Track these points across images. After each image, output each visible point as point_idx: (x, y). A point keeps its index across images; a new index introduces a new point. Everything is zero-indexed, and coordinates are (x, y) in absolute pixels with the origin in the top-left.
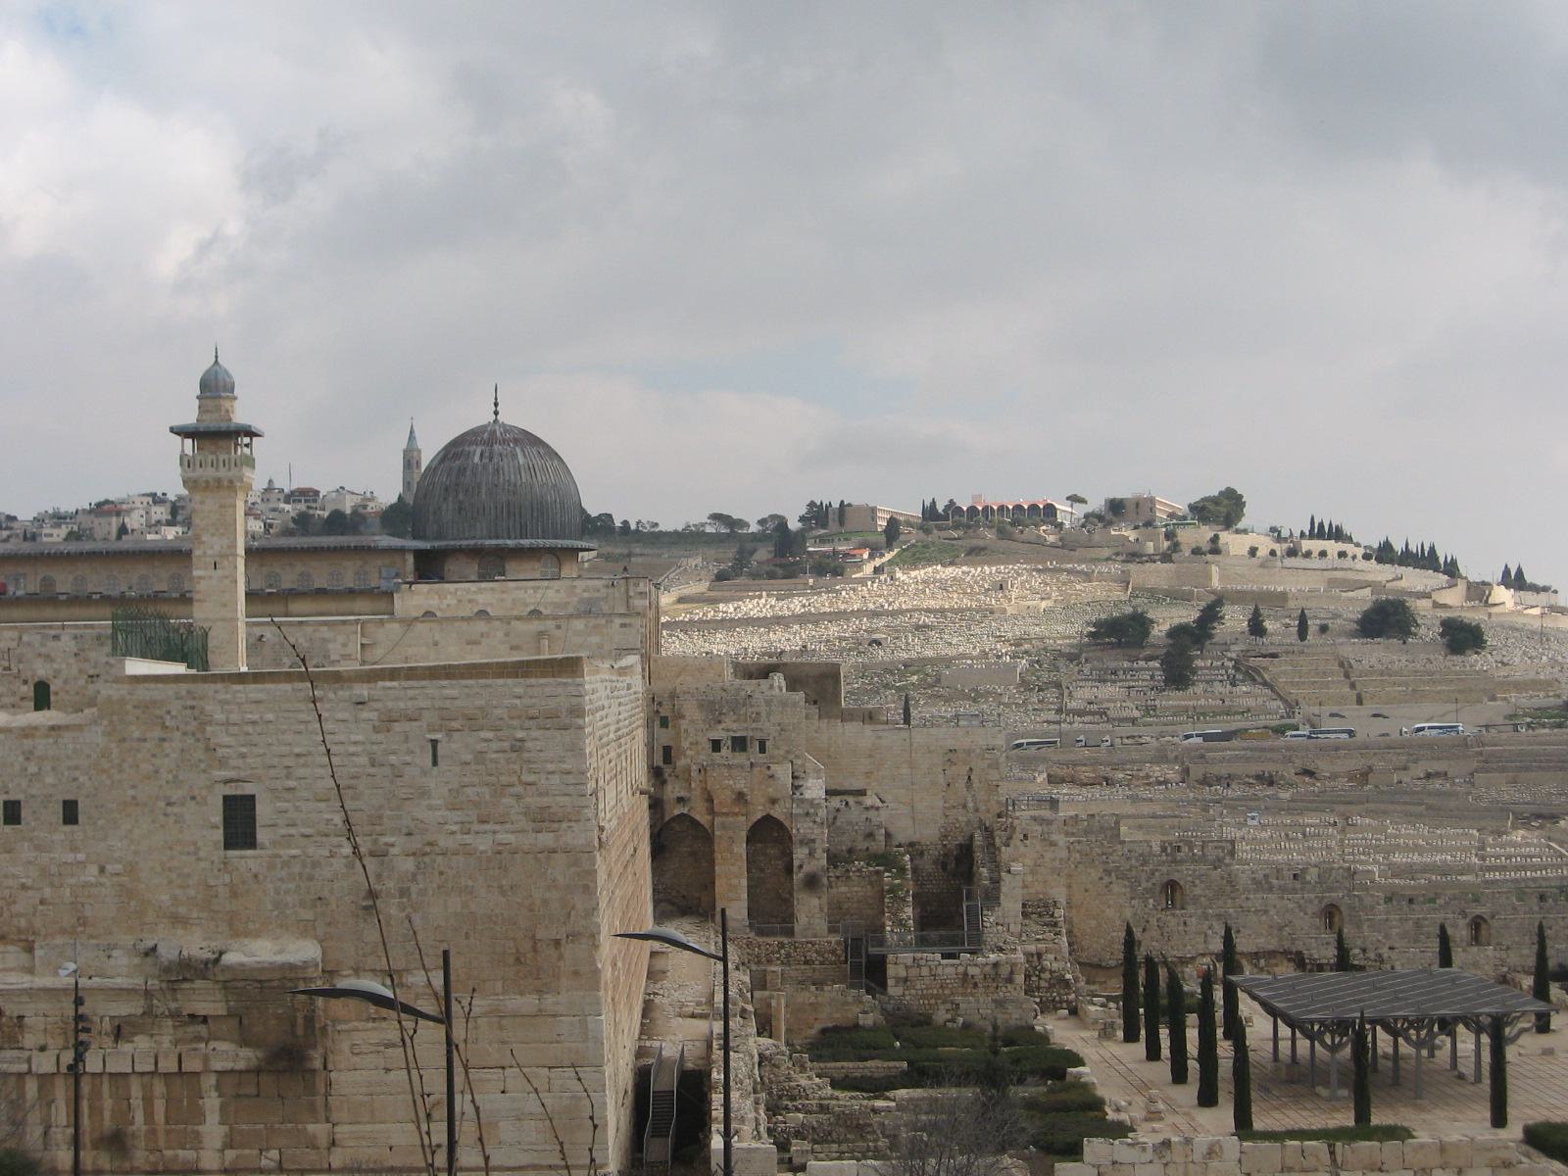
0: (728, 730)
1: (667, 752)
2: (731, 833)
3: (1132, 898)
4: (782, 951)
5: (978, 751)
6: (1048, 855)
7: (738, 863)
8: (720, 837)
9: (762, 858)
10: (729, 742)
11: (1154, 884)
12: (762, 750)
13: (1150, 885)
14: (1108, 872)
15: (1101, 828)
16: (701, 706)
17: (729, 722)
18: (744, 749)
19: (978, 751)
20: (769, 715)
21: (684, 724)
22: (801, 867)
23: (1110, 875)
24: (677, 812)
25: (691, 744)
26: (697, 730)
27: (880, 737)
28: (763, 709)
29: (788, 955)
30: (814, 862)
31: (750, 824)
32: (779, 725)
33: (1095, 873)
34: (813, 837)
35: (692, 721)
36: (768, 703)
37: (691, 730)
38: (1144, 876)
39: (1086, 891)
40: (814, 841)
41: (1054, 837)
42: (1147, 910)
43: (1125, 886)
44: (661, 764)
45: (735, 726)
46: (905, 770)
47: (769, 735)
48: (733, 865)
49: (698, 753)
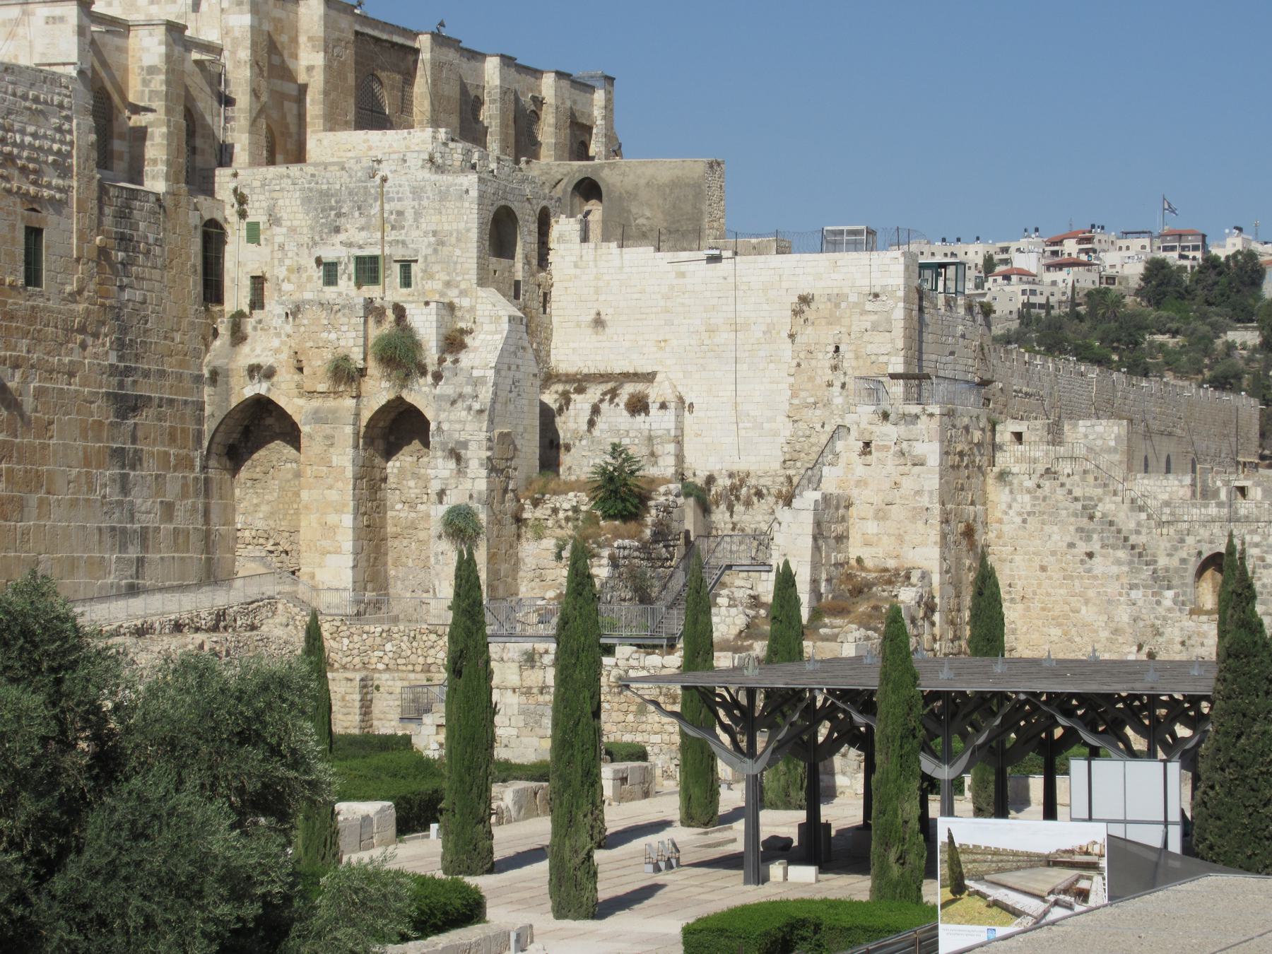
0: (350, 245)
1: (258, 282)
2: (327, 429)
3: (1133, 587)
4: (388, 647)
5: (853, 298)
6: (908, 484)
7: (340, 484)
8: (310, 437)
9: (412, 483)
10: (352, 267)
11: (1183, 561)
12: (406, 281)
13: (1175, 562)
14: (1085, 534)
15: (1090, 449)
16: (307, 201)
17: (352, 232)
18: (374, 280)
19: (853, 298)
20: (418, 215)
21: (279, 234)
22: (441, 494)
23: (1088, 539)
24: (251, 390)
25: (290, 270)
26: (300, 245)
27: (682, 275)
28: (408, 205)
29: (398, 654)
30: (467, 485)
31: (366, 416)
32: (435, 233)
33: (1058, 536)
34: (463, 437)
35: (292, 230)
36: (417, 192)
37: (291, 247)
38: (1164, 544)
39: (1043, 569)
40: (465, 445)
41: (920, 449)
42: (1161, 611)
43: (1118, 562)
44: (246, 310)
45: (360, 237)
46: (724, 337)
47: (417, 251)
48: (330, 488)
49: (300, 287)
